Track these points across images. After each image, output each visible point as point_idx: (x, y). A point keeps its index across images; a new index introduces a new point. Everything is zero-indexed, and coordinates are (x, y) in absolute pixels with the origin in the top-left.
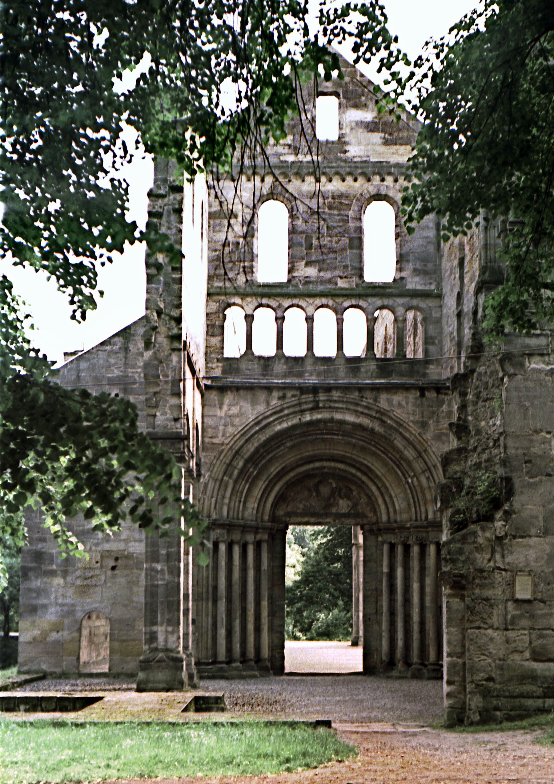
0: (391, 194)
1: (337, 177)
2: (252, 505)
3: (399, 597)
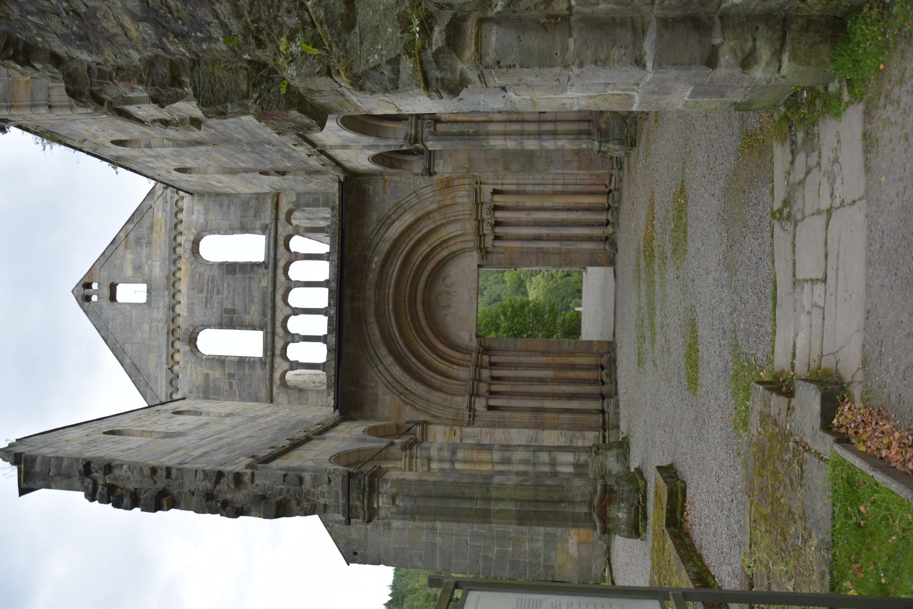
0: (192, 238)
1: (176, 285)
2: (455, 371)
3: (544, 231)
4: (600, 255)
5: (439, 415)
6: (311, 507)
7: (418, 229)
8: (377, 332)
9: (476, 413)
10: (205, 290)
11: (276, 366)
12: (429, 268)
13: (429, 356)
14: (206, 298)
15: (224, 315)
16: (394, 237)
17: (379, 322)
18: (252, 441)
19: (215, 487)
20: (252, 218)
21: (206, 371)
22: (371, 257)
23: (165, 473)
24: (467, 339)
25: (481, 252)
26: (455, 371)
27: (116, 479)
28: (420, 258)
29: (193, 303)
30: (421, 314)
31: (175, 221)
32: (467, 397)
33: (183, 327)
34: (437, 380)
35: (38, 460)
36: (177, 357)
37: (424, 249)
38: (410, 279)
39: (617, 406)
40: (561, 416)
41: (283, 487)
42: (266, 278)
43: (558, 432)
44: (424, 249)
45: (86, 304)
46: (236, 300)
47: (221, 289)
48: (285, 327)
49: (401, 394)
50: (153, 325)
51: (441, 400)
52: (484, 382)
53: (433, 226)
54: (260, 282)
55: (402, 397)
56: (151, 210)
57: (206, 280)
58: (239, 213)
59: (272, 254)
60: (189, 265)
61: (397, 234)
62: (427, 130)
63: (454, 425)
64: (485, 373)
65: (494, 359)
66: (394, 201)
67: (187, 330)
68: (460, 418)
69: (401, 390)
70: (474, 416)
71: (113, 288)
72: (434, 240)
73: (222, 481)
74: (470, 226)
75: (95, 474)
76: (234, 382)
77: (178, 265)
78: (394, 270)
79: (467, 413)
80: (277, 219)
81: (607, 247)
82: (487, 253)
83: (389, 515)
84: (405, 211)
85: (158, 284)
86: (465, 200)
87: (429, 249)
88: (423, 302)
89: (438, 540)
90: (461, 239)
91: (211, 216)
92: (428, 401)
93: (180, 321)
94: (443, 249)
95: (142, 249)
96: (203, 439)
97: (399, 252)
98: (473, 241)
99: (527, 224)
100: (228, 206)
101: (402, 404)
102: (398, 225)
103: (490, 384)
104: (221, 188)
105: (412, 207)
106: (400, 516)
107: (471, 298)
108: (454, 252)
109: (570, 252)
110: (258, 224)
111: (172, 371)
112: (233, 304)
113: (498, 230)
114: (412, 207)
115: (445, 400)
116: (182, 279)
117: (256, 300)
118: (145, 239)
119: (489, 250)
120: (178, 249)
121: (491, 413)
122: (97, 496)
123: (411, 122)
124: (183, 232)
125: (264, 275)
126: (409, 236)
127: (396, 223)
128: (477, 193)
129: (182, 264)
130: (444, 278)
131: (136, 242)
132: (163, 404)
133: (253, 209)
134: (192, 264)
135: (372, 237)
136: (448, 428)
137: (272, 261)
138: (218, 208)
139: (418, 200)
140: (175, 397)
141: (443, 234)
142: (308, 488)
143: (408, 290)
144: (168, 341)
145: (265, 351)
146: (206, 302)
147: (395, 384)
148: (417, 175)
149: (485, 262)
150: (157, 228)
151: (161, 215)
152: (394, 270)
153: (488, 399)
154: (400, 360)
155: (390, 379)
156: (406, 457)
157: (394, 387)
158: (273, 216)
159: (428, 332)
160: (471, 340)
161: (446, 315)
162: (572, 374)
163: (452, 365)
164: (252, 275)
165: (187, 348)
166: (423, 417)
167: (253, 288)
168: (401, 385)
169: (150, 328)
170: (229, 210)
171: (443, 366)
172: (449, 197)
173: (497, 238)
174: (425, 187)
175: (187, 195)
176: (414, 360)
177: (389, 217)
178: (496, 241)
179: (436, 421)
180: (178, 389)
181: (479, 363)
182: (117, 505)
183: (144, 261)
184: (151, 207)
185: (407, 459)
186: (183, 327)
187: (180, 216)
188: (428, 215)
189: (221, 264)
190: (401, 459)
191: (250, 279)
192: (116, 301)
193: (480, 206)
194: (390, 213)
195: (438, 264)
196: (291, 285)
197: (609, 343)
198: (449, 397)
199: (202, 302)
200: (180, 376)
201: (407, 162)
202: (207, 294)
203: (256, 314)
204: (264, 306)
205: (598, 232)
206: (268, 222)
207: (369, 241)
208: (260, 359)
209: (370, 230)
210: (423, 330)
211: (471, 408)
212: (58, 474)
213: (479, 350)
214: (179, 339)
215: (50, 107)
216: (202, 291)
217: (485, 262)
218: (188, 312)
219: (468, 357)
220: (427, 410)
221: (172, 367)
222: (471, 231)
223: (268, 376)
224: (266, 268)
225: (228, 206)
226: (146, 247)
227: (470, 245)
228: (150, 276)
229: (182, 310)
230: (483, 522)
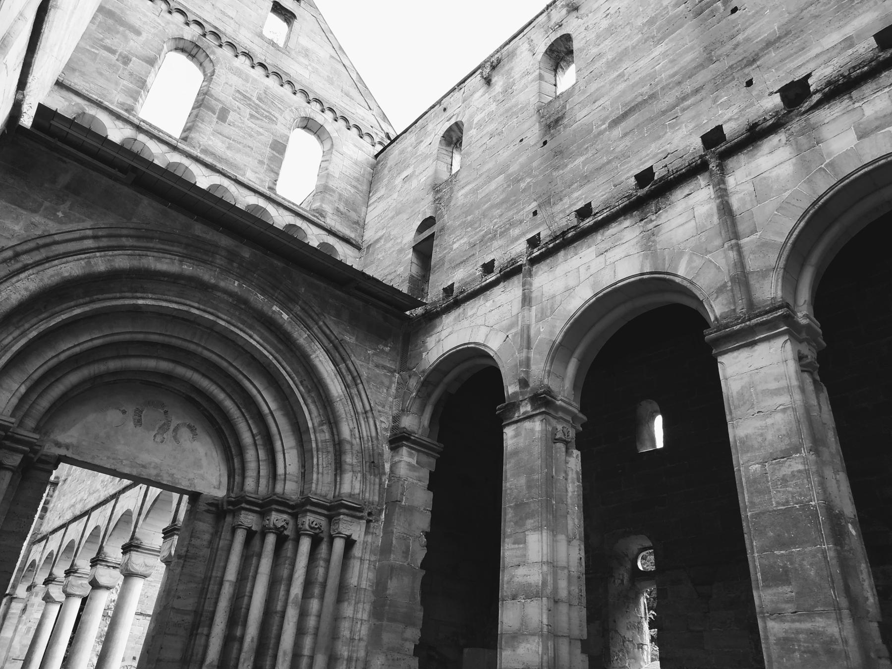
7: (309, 401)
11: (119, 124)
13: (67, 347)
14: (250, 99)
15: (220, 106)
16: (313, 356)
20: (336, 205)
21: (144, 35)
24: (62, 438)
25: (230, 503)
28: (254, 392)
29: (247, 80)
30: (151, 363)
37: (268, 402)
38: (225, 364)
44: (268, 402)
46: (237, 130)
49: (17, 255)
54: (253, 171)
57: (271, 111)
60: (296, 105)
61: (317, 362)
62: (560, 427)
66: (364, 373)
67: (214, 53)
69: (27, 259)
72: (280, 424)
74: (290, 489)
76: (114, 58)
78: (254, 340)
84: (347, 386)
86: (346, 488)
88: (168, 376)
94: (253, 436)
97: (280, 359)
98: (257, 492)
100: (355, 187)
102: (329, 369)
105: (352, 399)
107: (144, 466)
108: (233, 459)
113: (271, 539)
114: (352, 399)
119: (229, 519)
123: (571, 405)
127: (333, 367)
128: (356, 511)
130: (192, 429)
135: (321, 323)
139: (359, 411)
143: (206, 354)
146: (245, 96)
148: (396, 419)
149: (202, 506)
151: (360, 114)
152: (254, 340)
155: (61, 249)
159: (113, 365)
160: (58, 445)
161: (124, 412)
163: (28, 384)
170: (350, 185)
171: (36, 367)
172: (355, 461)
174: (376, 429)
177: (343, 359)
178: (245, 532)
184: (370, 109)
186: (219, 51)
188: (332, 421)
191: (261, 162)
193: (325, 512)
194: (349, 363)
201: (422, 410)
202: (254, 102)
203: (210, 143)
204: (220, 159)
207: (316, 317)
210: (118, 357)
213: (36, 452)
216: (259, 99)
219: (31, 423)
222: (279, 489)
223: (106, 103)
224: (270, 188)
227: (250, 485)
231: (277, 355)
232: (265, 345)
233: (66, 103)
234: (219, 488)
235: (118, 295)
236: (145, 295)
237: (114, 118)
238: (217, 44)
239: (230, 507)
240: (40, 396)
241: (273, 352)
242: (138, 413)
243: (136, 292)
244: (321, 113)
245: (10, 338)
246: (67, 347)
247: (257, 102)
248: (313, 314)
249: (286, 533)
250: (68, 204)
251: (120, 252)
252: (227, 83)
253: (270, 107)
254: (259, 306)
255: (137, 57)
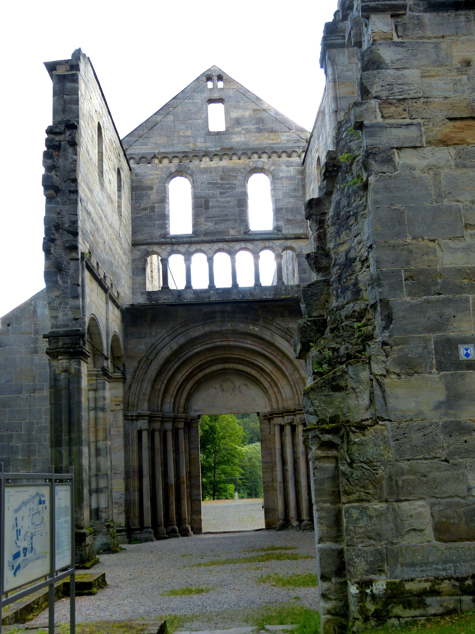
0: (266, 167)
1: (225, 156)
3: (290, 467)
4: (274, 516)
5: (132, 391)
6: (55, 307)
7: (285, 362)
8: (197, 334)
9: (135, 421)
10: (223, 182)
11: (164, 247)
12: (253, 372)
13: (180, 378)
14: (216, 183)
15: (203, 200)
16: (276, 343)
17: (205, 335)
18: (101, 246)
19: (65, 230)
20: (286, 217)
21: (155, 187)
22: (258, 325)
23: (73, 189)
25: (270, 415)
26: (169, 401)
27: (65, 150)
28: (260, 365)
29: (211, 172)
30: (214, 368)
31: (280, 151)
32: (148, 413)
33: (191, 165)
34: (161, 386)
35: (74, 85)
36: (166, 161)
37: (268, 367)
39: (146, 540)
40: (137, 493)
41: (69, 284)
42: (237, 234)
43: (123, 491)
44: (268, 367)
45: (204, 79)
46: (216, 209)
47: (225, 195)
48: (197, 251)
49: (147, 358)
50: (191, 138)
51: (144, 391)
52: (161, 426)
53: (287, 374)
54: (233, 229)
55: (145, 359)
56: (287, 130)
57: (230, 182)
58: (290, 206)
59: (256, 237)
60: (243, 166)
63: (124, 404)
64: (169, 426)
65: (181, 433)
67: (189, 168)
68: (130, 408)
69: (151, 357)
70: (132, 420)
71: (220, 100)
72: (276, 375)
73: (70, 236)
75: (68, 133)
76: (148, 212)
77: (242, 158)
79: (135, 414)
80: (287, 239)
81: (281, 521)
82: (270, 420)
83: (52, 369)
85: (226, 140)
87: (269, 372)
89: (24, 395)
90: (279, 398)
91: (285, 183)
92: (143, 381)
93: (196, 162)
95: (254, 124)
96: (100, 205)
99: (294, 452)
100: (295, 197)
101: (139, 359)
102: (286, 346)
103: (160, 431)
104: (309, 191)
106: (53, 377)
107: (231, 409)
109: (275, 490)
110: (281, 223)
111: (153, 158)
112: (213, 207)
115: (144, 395)
116: (231, 161)
117: (217, 226)
118: (263, 126)
119: (272, 421)
120: (256, 156)
121: (135, 434)
122: (52, 136)
124: (271, 159)
125: (239, 231)
126: (278, 355)
127: (287, 344)
129: (244, 161)
130: (245, 385)
131: (259, 119)
132: (125, 155)
133: (293, 217)
134: (244, 169)
135: (275, 324)
136: (121, 399)
137: (251, 237)
138: (293, 188)
140: (131, 162)
141: (282, 383)
142: (70, 303)
144: (179, 152)
145: (175, 237)
147: (155, 352)
150: (272, 136)
153: (147, 430)
154: (176, 354)
156: (97, 371)
157: (152, 351)
158: (289, 236)
160: (196, 411)
161: (215, 388)
162: (173, 498)
163: (173, 397)
164: (238, 221)
165: (173, 170)
166: (129, 377)
167: (227, 223)
168: (155, 358)
169: (188, 137)
170: (292, 197)
171: (173, 390)
173: (282, 428)
175: (302, 160)
176: (176, 366)
178: (279, 426)
179: (127, 388)
180: (138, 164)
181: (177, 420)
182: (47, 155)
183: (245, 127)
184: (290, 130)
185: (96, 372)
186: (191, 165)
187: (284, 155)
189: (245, 194)
190: (95, 367)
192: (209, 103)
195: (257, 379)
196: (232, 253)
197: (201, 529)
198: (147, 398)
199: (213, 180)
200: (149, 165)
202: (219, 184)
203: (206, 227)
204: (213, 233)
205: (292, 513)
206: (284, 231)
207: (271, 323)
208: (169, 234)
209: (280, 323)
210: (201, 371)
211: (139, 417)
212: (65, 102)
213: (188, 419)
214: (181, 162)
215: (336, 111)
216: (222, 179)
217: (262, 418)
218: (204, 168)
220: (135, 380)
221: (157, 158)
223: (155, 241)
225: (295, 197)
226: (256, 128)
228: (232, 133)
229: (206, 163)
230: (51, 441)
231: (262, 346)
232: (255, 344)
233: (140, 252)
234: (266, 408)
235: (187, 351)
236: (197, 346)
237: (160, 246)
238: (188, 161)
239: (271, 417)
240: (180, 398)
241: (259, 345)
242: (221, 386)
243: (193, 346)
244: (259, 160)
245: (159, 386)
246: (180, 378)
247: (221, 182)
248: (269, 322)
249: (294, 424)
250: (154, 327)
251: (180, 336)
252: (202, 183)
253: (229, 180)
254: (243, 330)
255: (156, 203)
